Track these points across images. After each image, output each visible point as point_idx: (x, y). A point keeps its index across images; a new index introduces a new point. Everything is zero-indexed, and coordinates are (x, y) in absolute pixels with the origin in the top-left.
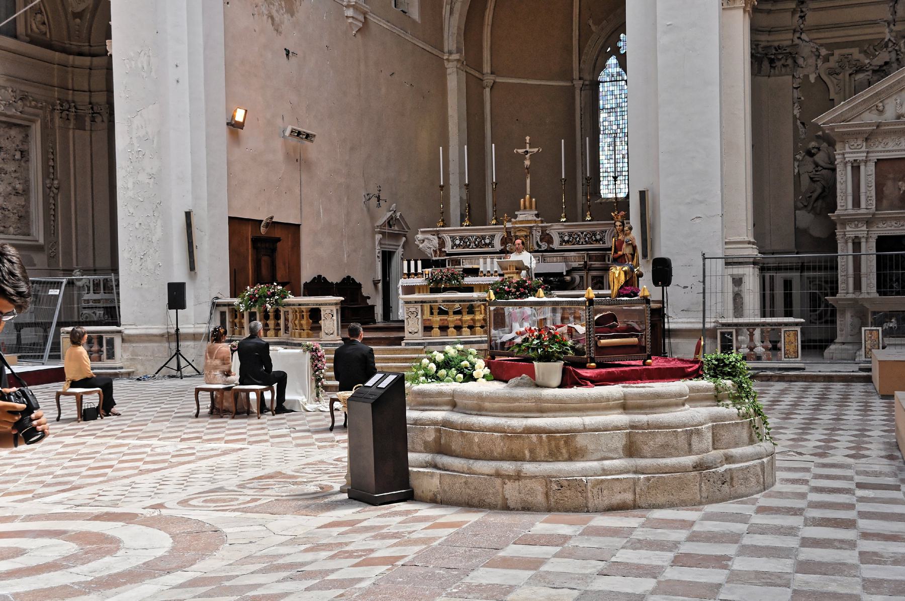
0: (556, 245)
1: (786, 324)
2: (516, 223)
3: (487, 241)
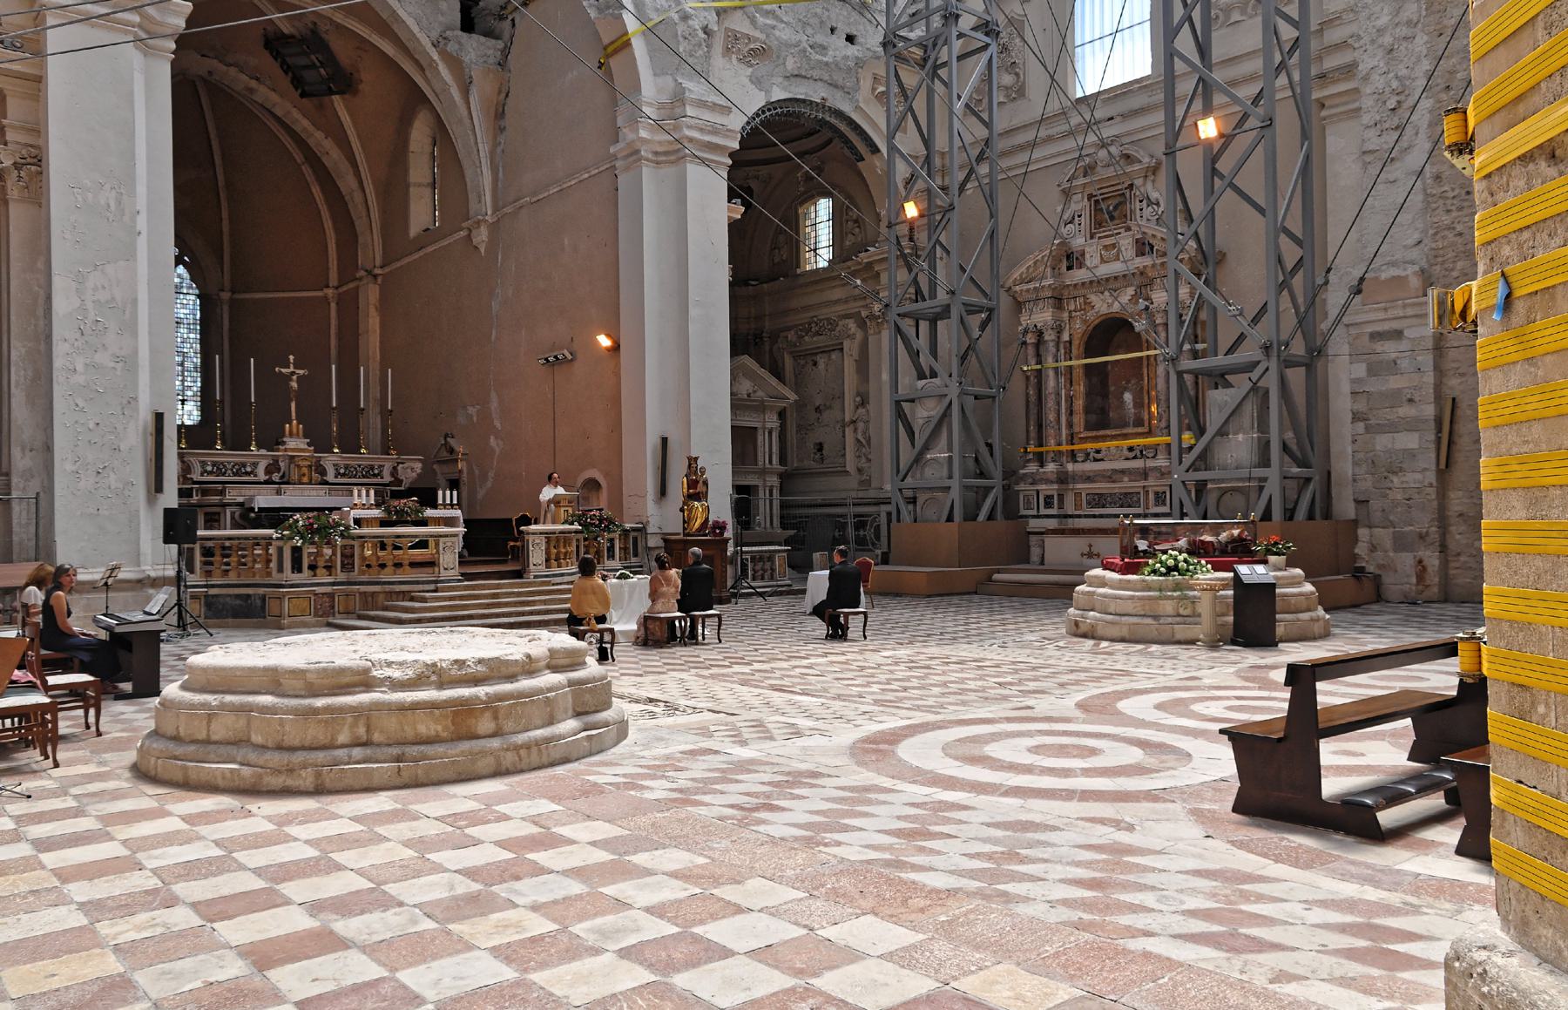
0: (330, 477)
1: (779, 551)
2: (286, 450)
3: (249, 469)
